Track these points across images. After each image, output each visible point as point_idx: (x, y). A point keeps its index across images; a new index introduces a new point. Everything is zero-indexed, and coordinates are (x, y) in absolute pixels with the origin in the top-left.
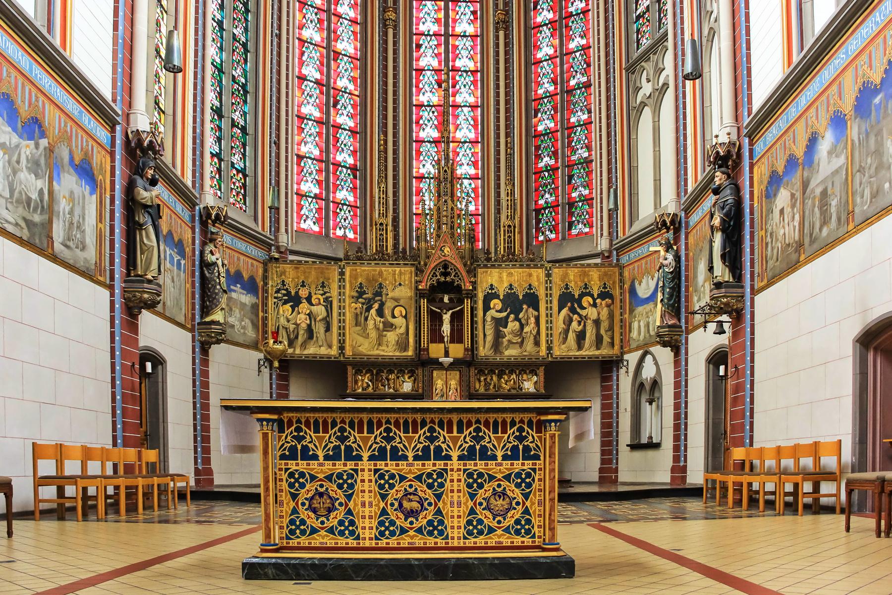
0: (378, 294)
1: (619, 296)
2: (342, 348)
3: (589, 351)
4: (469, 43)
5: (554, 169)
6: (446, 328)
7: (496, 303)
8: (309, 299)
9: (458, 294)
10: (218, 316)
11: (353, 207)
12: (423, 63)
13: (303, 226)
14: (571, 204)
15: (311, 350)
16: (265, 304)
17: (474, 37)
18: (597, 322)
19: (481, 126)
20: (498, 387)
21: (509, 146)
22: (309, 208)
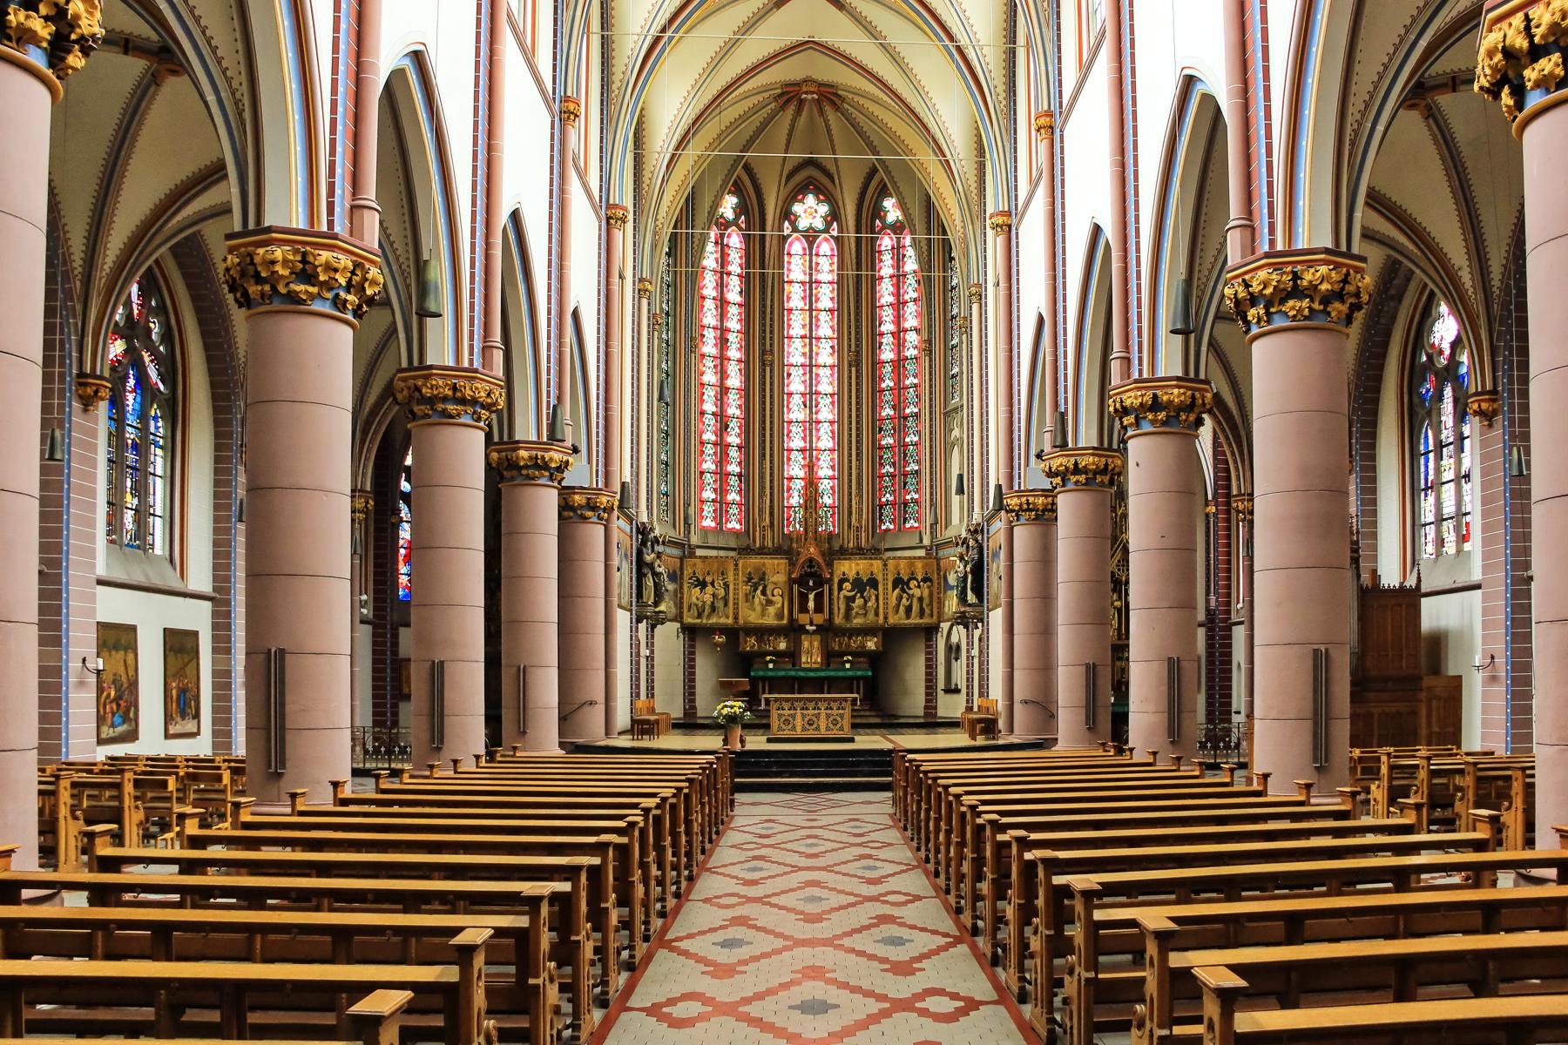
0: (762, 579)
1: (935, 578)
2: (736, 618)
3: (914, 620)
4: (828, 371)
5: (893, 476)
6: (811, 604)
7: (847, 585)
8: (713, 584)
9: (820, 582)
10: (662, 607)
11: (739, 505)
12: (792, 388)
13: (705, 523)
14: (906, 504)
15: (714, 620)
16: (681, 587)
17: (832, 367)
18: (921, 599)
19: (839, 438)
20: (848, 645)
21: (860, 468)
22: (708, 509)
